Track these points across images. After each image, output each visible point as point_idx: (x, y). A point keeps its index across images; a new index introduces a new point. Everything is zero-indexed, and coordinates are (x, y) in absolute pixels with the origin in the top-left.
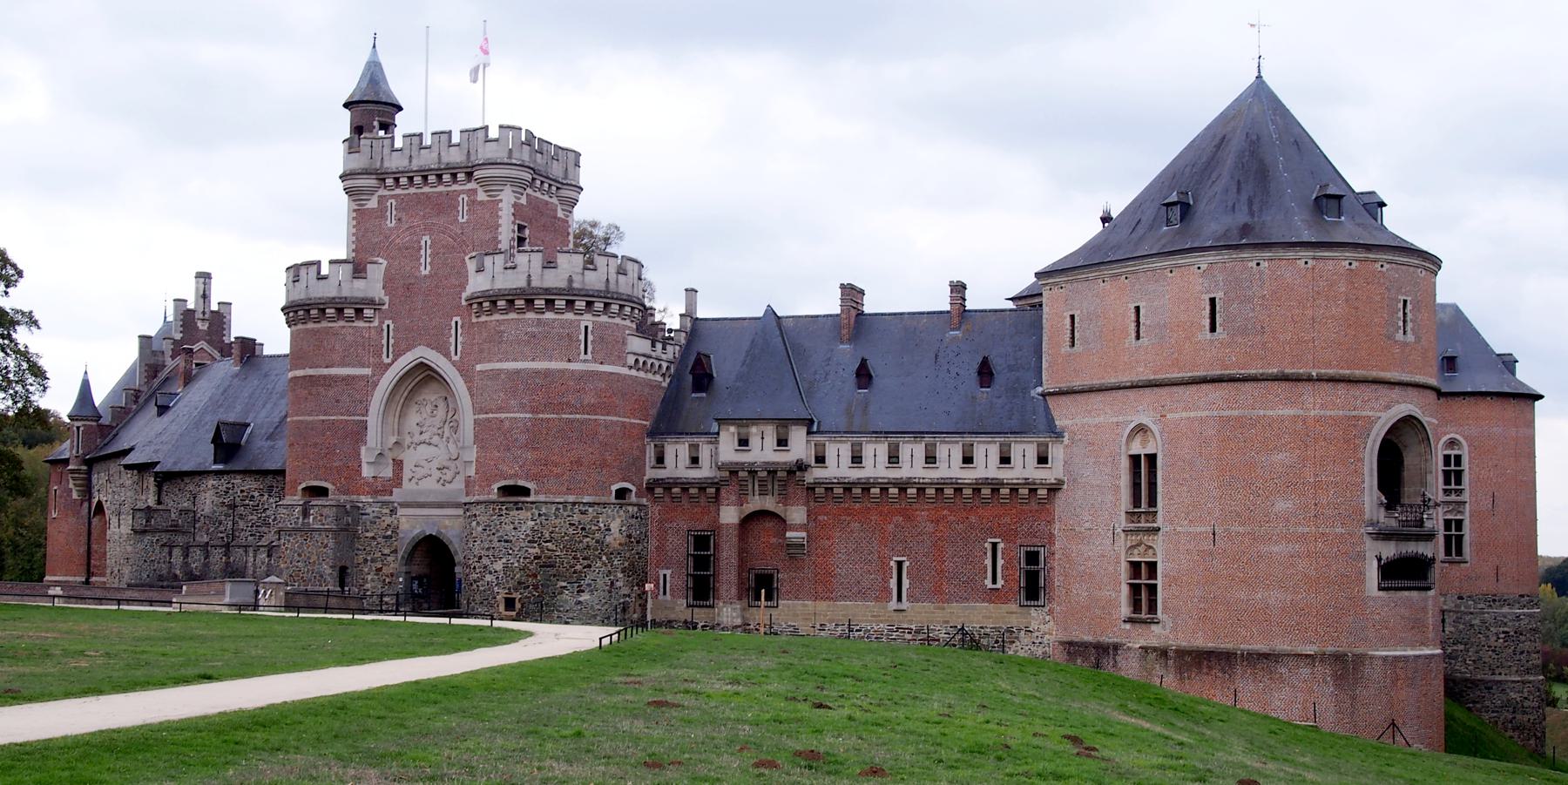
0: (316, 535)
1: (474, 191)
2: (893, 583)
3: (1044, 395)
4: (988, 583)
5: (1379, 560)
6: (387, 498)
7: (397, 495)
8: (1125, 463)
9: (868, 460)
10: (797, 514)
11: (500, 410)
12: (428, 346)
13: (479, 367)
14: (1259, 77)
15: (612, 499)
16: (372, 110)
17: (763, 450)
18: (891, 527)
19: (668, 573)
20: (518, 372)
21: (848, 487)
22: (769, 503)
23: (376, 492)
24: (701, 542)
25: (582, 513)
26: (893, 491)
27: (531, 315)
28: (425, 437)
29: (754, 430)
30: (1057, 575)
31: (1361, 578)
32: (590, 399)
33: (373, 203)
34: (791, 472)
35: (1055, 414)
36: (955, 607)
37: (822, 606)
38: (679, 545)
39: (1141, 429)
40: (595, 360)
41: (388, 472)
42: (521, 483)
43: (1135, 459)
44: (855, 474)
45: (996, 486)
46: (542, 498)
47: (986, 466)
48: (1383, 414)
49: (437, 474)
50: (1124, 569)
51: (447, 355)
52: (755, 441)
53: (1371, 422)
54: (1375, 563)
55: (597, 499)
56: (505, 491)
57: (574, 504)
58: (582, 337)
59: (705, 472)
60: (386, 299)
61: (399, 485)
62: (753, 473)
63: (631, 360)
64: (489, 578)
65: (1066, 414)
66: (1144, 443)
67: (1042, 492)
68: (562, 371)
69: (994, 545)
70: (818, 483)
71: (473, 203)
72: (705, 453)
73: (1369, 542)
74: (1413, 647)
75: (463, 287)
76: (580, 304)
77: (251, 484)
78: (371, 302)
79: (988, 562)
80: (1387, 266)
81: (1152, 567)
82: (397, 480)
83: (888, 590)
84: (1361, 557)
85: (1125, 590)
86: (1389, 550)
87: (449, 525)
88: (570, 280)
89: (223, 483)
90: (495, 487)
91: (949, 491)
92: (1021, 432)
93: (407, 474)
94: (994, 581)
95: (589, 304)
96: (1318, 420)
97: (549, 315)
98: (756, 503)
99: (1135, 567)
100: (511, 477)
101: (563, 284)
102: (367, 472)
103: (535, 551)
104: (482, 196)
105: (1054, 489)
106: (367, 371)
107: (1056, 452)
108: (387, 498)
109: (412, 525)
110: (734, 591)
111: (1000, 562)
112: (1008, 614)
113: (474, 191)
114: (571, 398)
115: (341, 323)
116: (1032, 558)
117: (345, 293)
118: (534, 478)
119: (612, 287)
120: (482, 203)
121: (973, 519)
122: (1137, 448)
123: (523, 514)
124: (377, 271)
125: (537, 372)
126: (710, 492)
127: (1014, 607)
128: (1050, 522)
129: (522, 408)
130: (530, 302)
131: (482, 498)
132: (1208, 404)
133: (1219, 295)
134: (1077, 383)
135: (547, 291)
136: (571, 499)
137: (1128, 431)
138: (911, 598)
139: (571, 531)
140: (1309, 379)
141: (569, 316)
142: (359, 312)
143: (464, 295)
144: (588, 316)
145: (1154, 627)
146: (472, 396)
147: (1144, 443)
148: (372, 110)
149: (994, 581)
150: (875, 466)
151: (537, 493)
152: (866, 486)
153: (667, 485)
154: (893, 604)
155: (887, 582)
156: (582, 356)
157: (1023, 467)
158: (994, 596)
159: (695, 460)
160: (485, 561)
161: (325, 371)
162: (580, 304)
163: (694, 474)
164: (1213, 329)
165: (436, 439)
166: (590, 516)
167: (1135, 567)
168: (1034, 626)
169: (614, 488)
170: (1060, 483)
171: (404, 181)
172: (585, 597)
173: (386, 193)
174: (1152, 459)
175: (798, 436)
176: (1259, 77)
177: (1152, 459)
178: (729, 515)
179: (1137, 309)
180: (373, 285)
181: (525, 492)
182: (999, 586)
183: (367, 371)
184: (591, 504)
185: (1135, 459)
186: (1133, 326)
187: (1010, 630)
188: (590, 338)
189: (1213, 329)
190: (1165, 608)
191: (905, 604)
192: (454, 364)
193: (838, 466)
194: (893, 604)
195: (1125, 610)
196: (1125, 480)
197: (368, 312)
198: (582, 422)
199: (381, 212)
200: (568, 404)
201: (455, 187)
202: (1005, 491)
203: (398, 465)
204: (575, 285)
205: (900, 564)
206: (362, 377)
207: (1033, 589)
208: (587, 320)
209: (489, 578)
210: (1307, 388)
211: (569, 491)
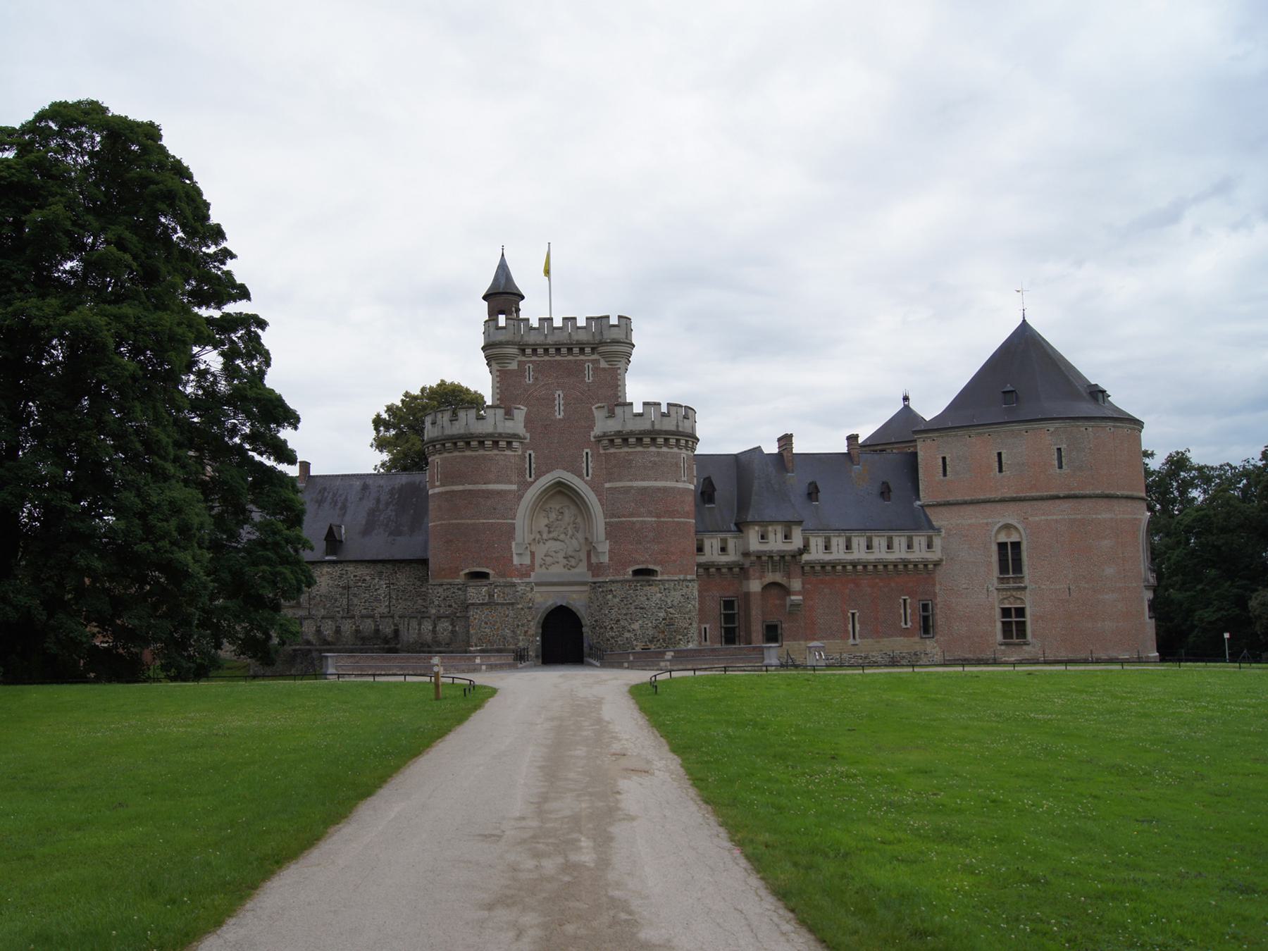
0: (499, 608)
1: (597, 361)
2: (850, 626)
3: (922, 506)
6: (527, 580)
7: (533, 578)
8: (995, 548)
9: (834, 548)
10: (796, 584)
11: (632, 515)
12: (564, 469)
13: (607, 485)
14: (1024, 321)
16: (503, 296)
17: (776, 543)
18: (847, 591)
19: (707, 626)
20: (645, 488)
21: (823, 565)
22: (778, 577)
23: (522, 576)
24: (728, 604)
26: (850, 567)
27: (653, 449)
28: (554, 535)
29: (770, 528)
30: (939, 619)
33: (513, 366)
34: (794, 556)
35: (932, 518)
36: (885, 641)
38: (716, 609)
39: (1007, 527)
41: (527, 561)
42: (651, 567)
43: (1002, 546)
44: (827, 557)
45: (906, 563)
46: (666, 577)
47: (900, 552)
49: (565, 561)
50: (998, 612)
51: (580, 476)
52: (771, 536)
56: (636, 573)
59: (731, 557)
60: (528, 435)
61: (533, 570)
64: (627, 635)
65: (939, 518)
66: (1008, 536)
67: (931, 566)
68: (673, 489)
70: (807, 563)
71: (596, 369)
72: (731, 545)
75: (591, 428)
77: (362, 571)
78: (516, 436)
81: (1021, 612)
82: (532, 567)
83: (847, 631)
85: (999, 625)
87: (576, 599)
89: (337, 571)
90: (630, 571)
91: (880, 567)
92: (917, 527)
93: (538, 561)
97: (665, 449)
98: (771, 577)
99: (1006, 612)
100: (643, 563)
101: (673, 428)
102: (516, 561)
103: (662, 615)
104: (603, 364)
105: (937, 564)
106: (514, 487)
107: (937, 542)
108: (527, 580)
109: (545, 599)
110: (760, 637)
111: (909, 611)
112: (913, 643)
113: (597, 361)
115: (496, 452)
116: (925, 607)
117: (500, 430)
118: (661, 563)
120: (604, 369)
121: (893, 585)
122: (1003, 538)
123: (654, 589)
124: (520, 414)
125: (658, 489)
126: (741, 571)
127: (917, 639)
128: (934, 585)
129: (650, 514)
130: (654, 440)
131: (618, 578)
132: (1060, 513)
133: (1063, 446)
134: (951, 499)
135: (667, 432)
136: (682, 577)
137: (997, 527)
138: (861, 637)
140: (1118, 497)
142: (509, 443)
143: (592, 434)
145: (1025, 648)
146: (602, 505)
147: (1008, 536)
148: (503, 296)
150: (838, 552)
151: (662, 574)
152: (834, 565)
153: (706, 567)
154: (851, 641)
155: (846, 626)
157: (919, 553)
158: (906, 633)
159: (723, 549)
160: (622, 623)
161: (484, 487)
163: (724, 559)
164: (1060, 467)
165: (562, 537)
167: (1006, 612)
168: (928, 650)
170: (941, 560)
171: (540, 351)
173: (524, 359)
174: (1016, 546)
175: (797, 534)
176: (1024, 321)
177: (1016, 546)
178: (755, 586)
179: (1000, 454)
180: (517, 425)
181: (650, 572)
183: (514, 487)
185: (1002, 546)
186: (996, 464)
187: (915, 654)
189: (1060, 467)
190: (1034, 636)
191: (858, 641)
192: (586, 482)
193: (816, 553)
194: (851, 641)
195: (999, 637)
196: (995, 558)
197: (515, 444)
199: (521, 371)
201: (582, 357)
202: (911, 566)
203: (533, 554)
205: (853, 614)
206: (510, 491)
207: (926, 627)
209: (627, 635)
210: (1115, 502)
211: (680, 572)
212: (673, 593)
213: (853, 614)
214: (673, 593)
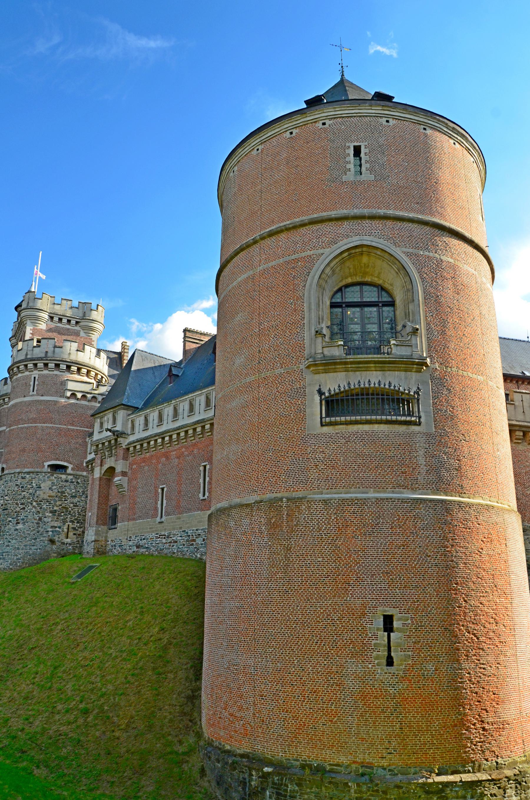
4: (201, 496)
5: (320, 393)
15: (46, 469)
25: (23, 478)
31: (301, 415)
32: (32, 415)
37: (131, 523)
40: (38, 394)
48: (327, 251)
53: (311, 261)
54: (317, 398)
55: (32, 470)
57: (19, 473)
58: (32, 383)
62: (103, 444)
63: (69, 394)
68: (21, 402)
69: (205, 467)
73: (309, 377)
74: (378, 488)
76: (30, 366)
79: (201, 481)
80: (328, 122)
83: (156, 509)
84: (301, 393)
86: (335, 382)
88: (27, 355)
94: (204, 495)
95: (35, 365)
96: (262, 273)
97: (20, 375)
98: (109, 463)
101: (23, 357)
114: (23, 416)
119: (49, 354)
121: (195, 451)
136: (18, 470)
138: (168, 514)
139: (16, 489)
141: (27, 373)
144: (36, 372)
149: (204, 495)
154: (158, 519)
155: (156, 503)
156: (31, 393)
162: (30, 366)
166: (27, 480)
169: (46, 464)
172: (20, 526)
178: (97, 474)
182: (206, 497)
184: (28, 473)
188: (36, 383)
198: (27, 428)
200: (21, 419)
204: (29, 357)
205: (163, 489)
208: (36, 374)
211: (18, 466)
212: (10, 484)
213: (163, 489)
214: (10, 484)
